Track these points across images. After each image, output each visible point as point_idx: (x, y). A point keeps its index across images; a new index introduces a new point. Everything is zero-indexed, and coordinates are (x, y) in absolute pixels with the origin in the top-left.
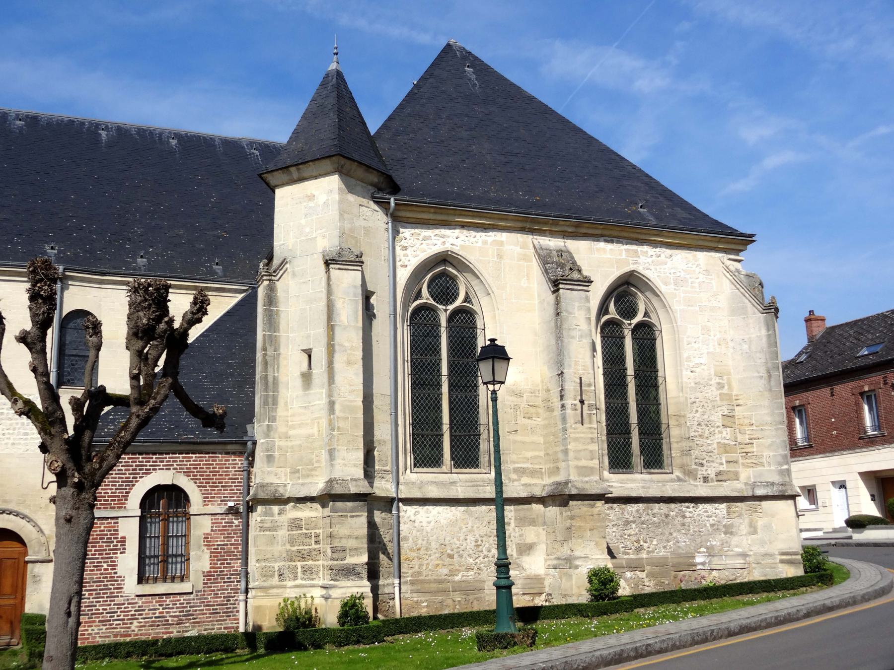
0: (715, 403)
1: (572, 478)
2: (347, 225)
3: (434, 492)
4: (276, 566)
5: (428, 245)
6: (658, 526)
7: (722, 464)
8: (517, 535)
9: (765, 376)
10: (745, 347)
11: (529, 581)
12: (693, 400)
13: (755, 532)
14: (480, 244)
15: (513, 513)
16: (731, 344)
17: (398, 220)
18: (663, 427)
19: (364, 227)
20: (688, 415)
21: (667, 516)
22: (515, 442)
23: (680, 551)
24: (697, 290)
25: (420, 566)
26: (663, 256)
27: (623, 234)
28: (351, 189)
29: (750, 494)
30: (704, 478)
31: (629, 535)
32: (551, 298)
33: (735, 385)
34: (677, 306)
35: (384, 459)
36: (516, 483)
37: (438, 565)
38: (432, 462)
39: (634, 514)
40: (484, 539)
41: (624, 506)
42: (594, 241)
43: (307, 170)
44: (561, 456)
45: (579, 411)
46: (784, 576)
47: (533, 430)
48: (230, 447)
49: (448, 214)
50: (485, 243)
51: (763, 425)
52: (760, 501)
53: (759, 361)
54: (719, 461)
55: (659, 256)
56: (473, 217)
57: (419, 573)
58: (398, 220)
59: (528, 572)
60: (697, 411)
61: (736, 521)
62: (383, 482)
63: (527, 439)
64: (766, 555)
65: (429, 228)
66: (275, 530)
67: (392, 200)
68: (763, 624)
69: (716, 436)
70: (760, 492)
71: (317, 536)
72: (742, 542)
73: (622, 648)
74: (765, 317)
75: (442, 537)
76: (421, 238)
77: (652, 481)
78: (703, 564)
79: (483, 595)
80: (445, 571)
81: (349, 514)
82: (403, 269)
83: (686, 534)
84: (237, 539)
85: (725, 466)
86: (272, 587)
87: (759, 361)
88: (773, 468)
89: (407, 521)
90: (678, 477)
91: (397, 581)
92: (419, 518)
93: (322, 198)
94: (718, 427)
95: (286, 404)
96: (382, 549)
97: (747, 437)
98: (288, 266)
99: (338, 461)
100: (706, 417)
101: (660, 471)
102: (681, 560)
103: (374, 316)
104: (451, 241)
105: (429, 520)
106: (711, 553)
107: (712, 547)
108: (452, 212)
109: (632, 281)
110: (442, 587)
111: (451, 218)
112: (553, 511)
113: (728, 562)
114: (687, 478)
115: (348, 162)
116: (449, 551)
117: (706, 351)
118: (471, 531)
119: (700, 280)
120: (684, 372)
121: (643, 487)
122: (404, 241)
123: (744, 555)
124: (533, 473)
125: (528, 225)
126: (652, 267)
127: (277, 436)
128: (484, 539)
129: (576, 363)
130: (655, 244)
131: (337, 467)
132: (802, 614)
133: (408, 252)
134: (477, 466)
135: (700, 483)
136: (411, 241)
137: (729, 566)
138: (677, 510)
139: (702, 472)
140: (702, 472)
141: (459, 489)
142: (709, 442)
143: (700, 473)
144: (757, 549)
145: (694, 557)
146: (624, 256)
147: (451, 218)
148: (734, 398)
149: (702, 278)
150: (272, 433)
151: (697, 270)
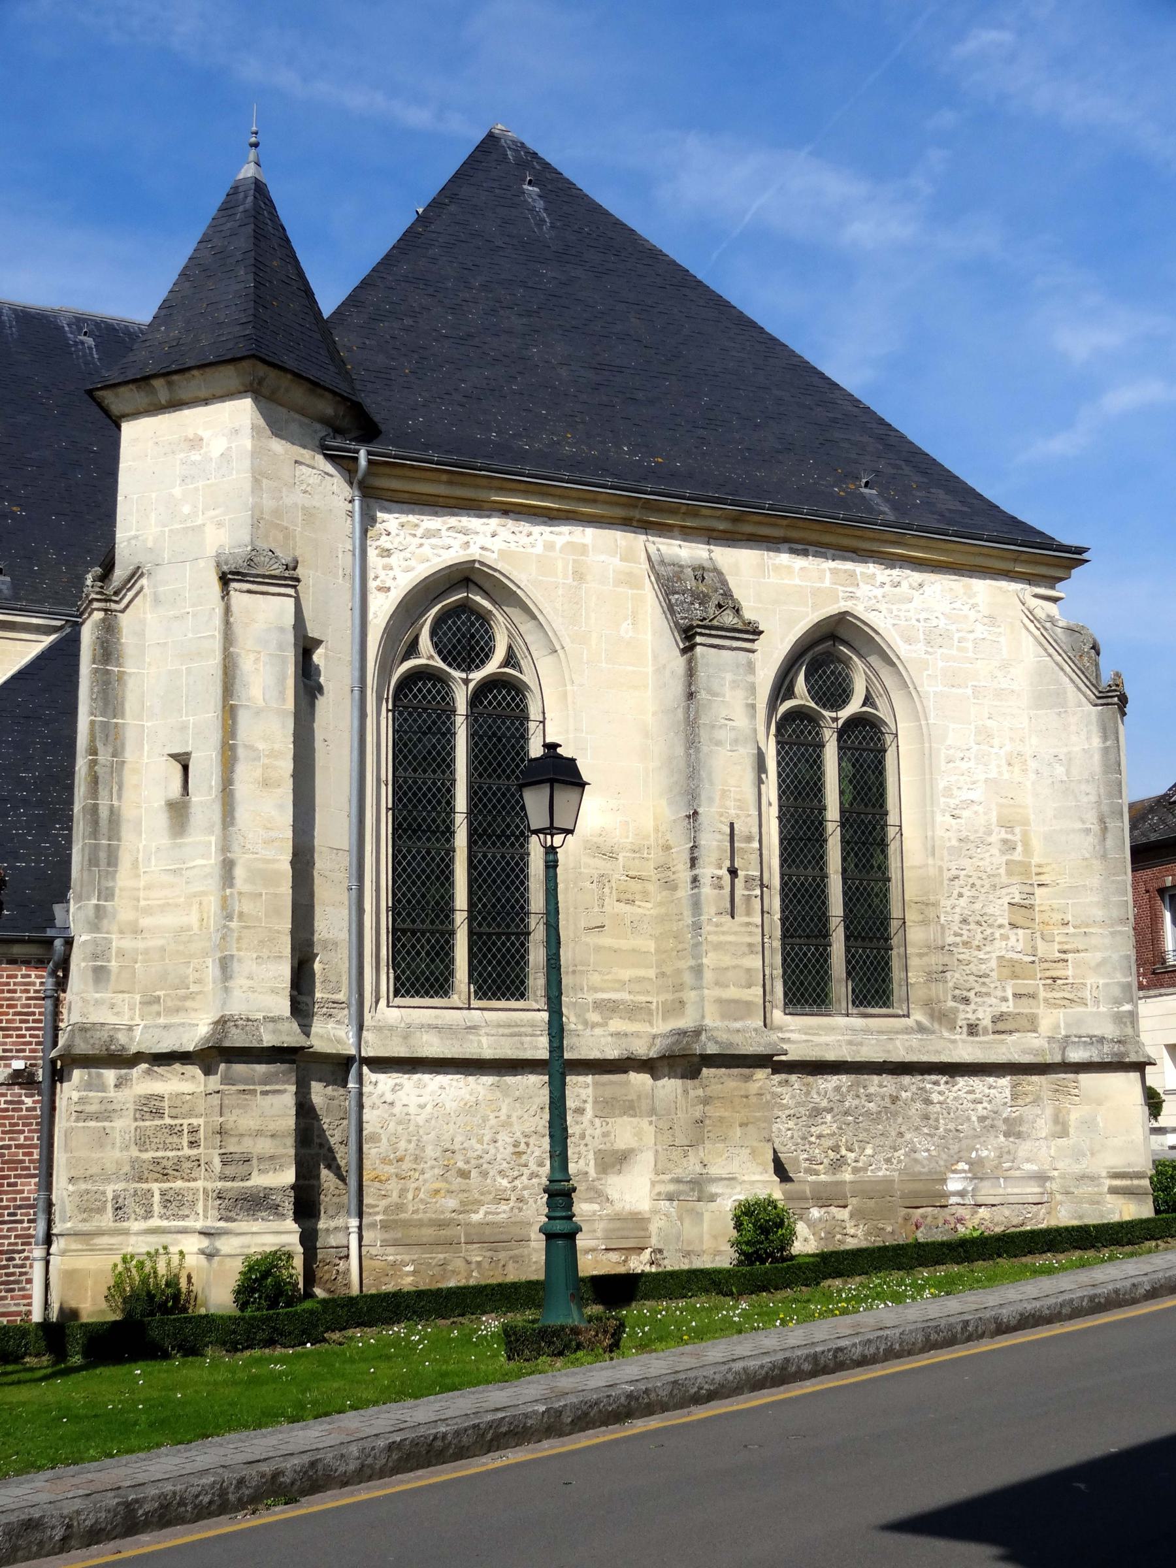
0: (997, 880)
1: (708, 1022)
2: (268, 503)
3: (432, 1047)
4: (110, 1190)
5: (433, 547)
6: (875, 1118)
7: (1005, 999)
8: (598, 1132)
9: (1096, 828)
10: (1060, 770)
11: (618, 1224)
12: (954, 872)
13: (1064, 1133)
14: (539, 549)
15: (590, 1091)
16: (1033, 765)
17: (373, 495)
18: (894, 924)
19: (304, 508)
20: (943, 903)
21: (895, 1099)
22: (598, 949)
23: (918, 1168)
24: (970, 654)
25: (403, 1192)
26: (905, 584)
27: (827, 538)
28: (277, 429)
29: (1057, 1059)
30: (970, 1026)
31: (819, 1137)
33: (1036, 843)
34: (929, 685)
35: (333, 979)
36: (598, 1031)
37: (437, 1192)
38: (432, 986)
39: (831, 1094)
40: (532, 1141)
41: (810, 1079)
42: (769, 550)
44: (688, 978)
45: (728, 889)
46: (1115, 1218)
47: (634, 927)
48: (17, 950)
49: (477, 487)
50: (550, 546)
51: (1087, 926)
52: (1077, 1072)
53: (1085, 799)
54: (999, 993)
55: (898, 585)
56: (526, 493)
57: (400, 1207)
58: (373, 495)
59: (618, 1207)
60: (961, 895)
61: (1029, 1112)
62: (331, 1025)
63: (624, 944)
64: (1083, 1177)
65: (436, 514)
66: (109, 1119)
67: (362, 454)
69: (997, 944)
71: (194, 1131)
72: (1039, 1152)
73: (788, 1354)
74: (1101, 713)
75: (447, 1136)
76: (419, 532)
77: (867, 1031)
78: (962, 1194)
79: (526, 1252)
80: (452, 1203)
81: (259, 1088)
82: (381, 596)
83: (931, 1136)
84: (30, 1136)
85: (1011, 1003)
86: (101, 1233)
87: (1085, 799)
88: (1102, 1009)
89: (378, 1102)
90: (918, 1023)
91: (354, 1223)
92: (402, 1097)
93: (217, 446)
94: (1000, 926)
95: (135, 864)
96: (325, 1159)
97: (1057, 947)
98: (144, 581)
99: (239, 982)
100: (978, 906)
101: (884, 1011)
102: (919, 1186)
103: (320, 689)
104: (481, 540)
105: (422, 1100)
106: (978, 1171)
107: (980, 1161)
108: (485, 482)
109: (842, 633)
110: (444, 1235)
111: (481, 495)
112: (670, 1087)
113: (1009, 1190)
114: (936, 1026)
115: (272, 374)
116: (460, 1164)
117: (982, 777)
118: (507, 1124)
119: (977, 635)
120: (939, 818)
121: (850, 1043)
122: (384, 538)
123: (1041, 1178)
124: (633, 1011)
125: (636, 514)
126: (883, 607)
127: (115, 928)
128: (532, 1141)
129: (724, 792)
130: (891, 561)
131: (237, 993)
132: (1141, 1291)
133: (393, 561)
134: (522, 996)
135: (961, 1036)
136: (401, 538)
137: (1012, 1199)
138: (914, 1088)
139: (965, 1015)
140: (965, 1015)
141: (484, 1040)
142: (981, 955)
143: (962, 1016)
144: (1067, 1166)
145: (944, 1181)
146: (827, 583)
147: (481, 495)
148: (1034, 870)
149: (980, 630)
150: (105, 922)
151: (973, 615)
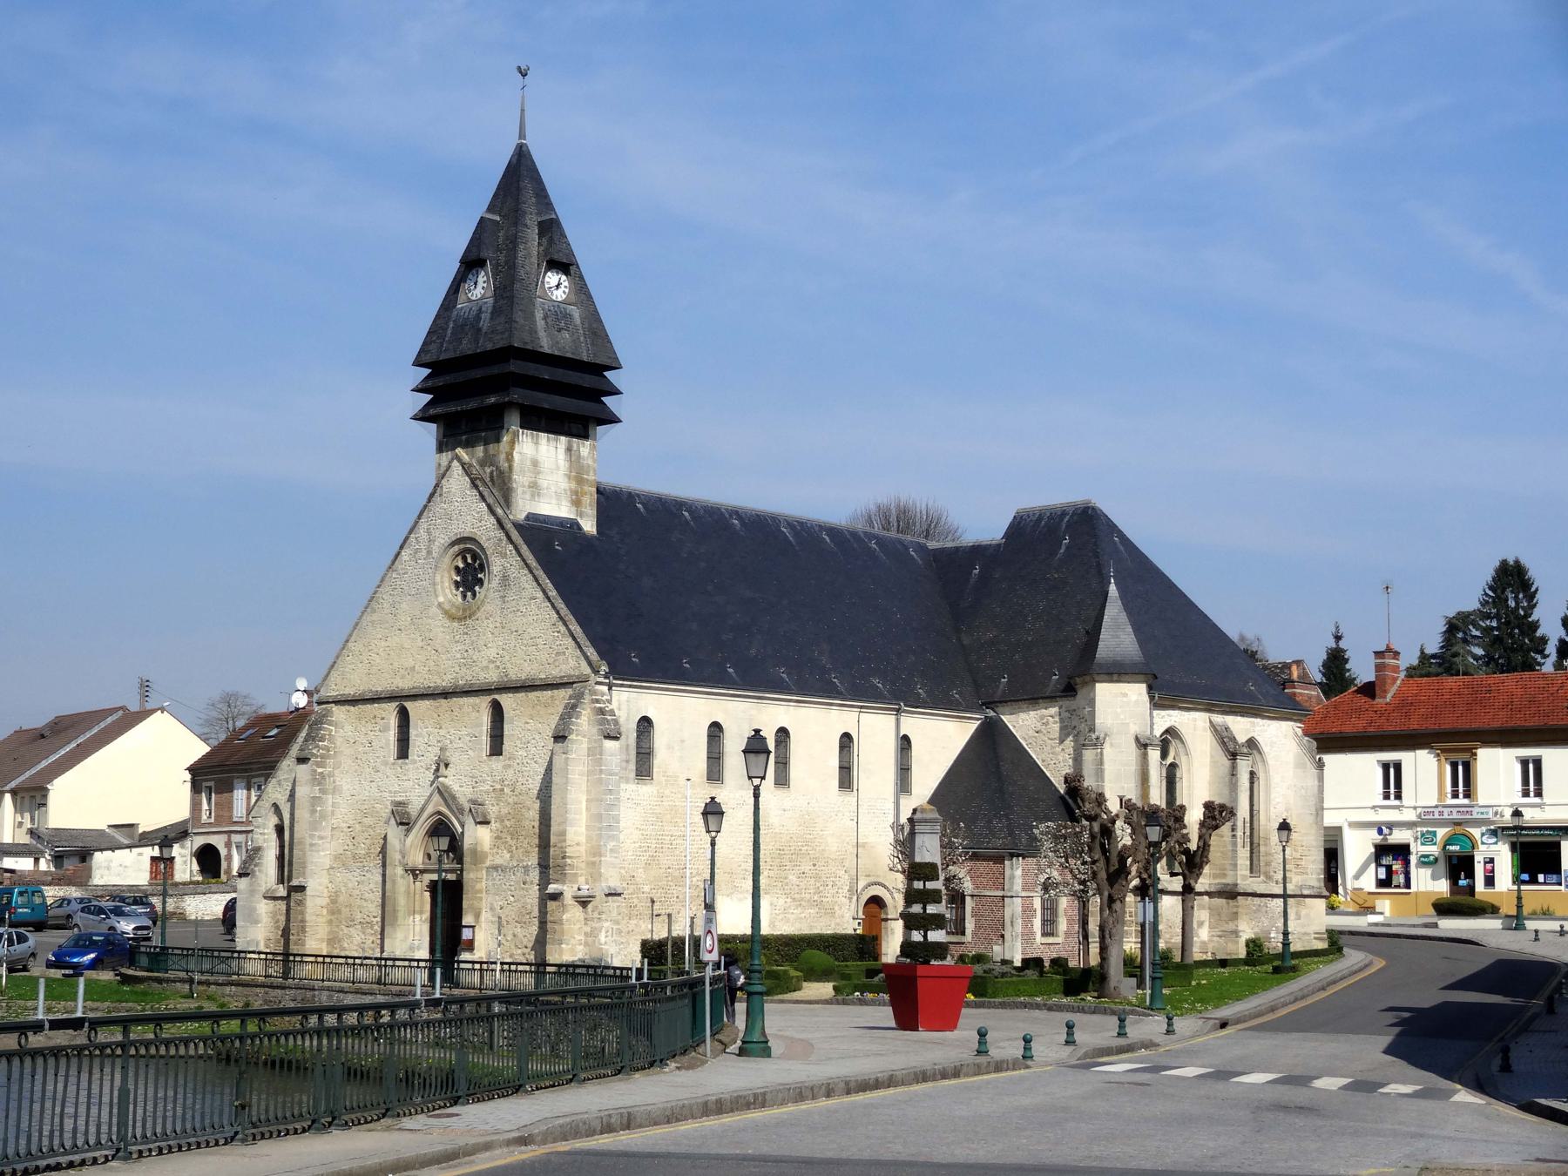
17: (1156, 704)
32: (1225, 762)
68: (583, 1128)
70: (1306, 892)
93: (1134, 698)
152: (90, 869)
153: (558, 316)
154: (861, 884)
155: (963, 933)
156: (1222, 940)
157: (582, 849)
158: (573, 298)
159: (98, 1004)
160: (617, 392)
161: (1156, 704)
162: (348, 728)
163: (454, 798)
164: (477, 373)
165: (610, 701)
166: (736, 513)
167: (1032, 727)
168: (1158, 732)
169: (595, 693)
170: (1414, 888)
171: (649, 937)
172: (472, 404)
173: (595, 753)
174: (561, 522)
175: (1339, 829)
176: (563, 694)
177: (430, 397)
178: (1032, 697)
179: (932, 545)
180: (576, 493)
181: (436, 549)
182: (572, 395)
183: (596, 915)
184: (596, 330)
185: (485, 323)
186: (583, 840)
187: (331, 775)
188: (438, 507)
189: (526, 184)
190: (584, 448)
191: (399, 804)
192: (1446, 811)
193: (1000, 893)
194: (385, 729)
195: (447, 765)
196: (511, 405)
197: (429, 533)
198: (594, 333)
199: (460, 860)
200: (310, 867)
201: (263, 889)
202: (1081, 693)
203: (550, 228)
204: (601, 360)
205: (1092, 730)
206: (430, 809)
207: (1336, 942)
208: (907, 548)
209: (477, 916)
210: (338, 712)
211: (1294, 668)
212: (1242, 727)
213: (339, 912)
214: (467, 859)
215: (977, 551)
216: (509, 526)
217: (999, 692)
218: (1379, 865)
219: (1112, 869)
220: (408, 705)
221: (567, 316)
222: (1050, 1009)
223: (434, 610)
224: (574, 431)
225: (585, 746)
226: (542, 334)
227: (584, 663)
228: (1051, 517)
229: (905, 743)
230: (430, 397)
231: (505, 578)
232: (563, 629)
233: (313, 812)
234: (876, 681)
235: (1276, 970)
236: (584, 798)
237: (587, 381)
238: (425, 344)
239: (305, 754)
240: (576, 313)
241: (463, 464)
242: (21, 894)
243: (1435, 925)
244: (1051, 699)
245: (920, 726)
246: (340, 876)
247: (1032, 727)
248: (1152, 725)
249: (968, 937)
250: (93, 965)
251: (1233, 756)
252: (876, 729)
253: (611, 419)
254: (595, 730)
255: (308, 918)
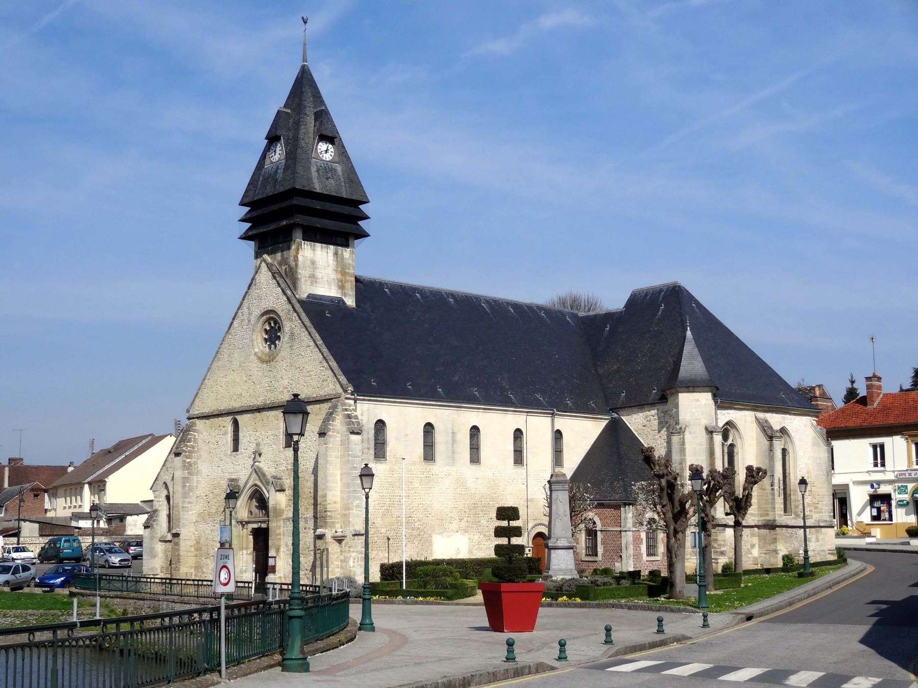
32: (768, 443)
43: (697, 389)
70: (822, 524)
93: (703, 402)
112: (763, 531)
130: (790, 414)
144: (818, 548)
152: (125, 526)
153: (327, 170)
154: (531, 525)
155: (596, 555)
156: (767, 556)
157: (338, 506)
158: (337, 159)
159: (35, 611)
160: (365, 217)
161: (720, 406)
162: (205, 433)
163: (264, 475)
164: (275, 207)
165: (355, 410)
166: (452, 295)
167: (641, 424)
168: (721, 424)
169: (345, 404)
170: (894, 521)
171: (386, 561)
172: (272, 227)
173: (345, 444)
174: (331, 299)
175: (847, 485)
176: (326, 406)
177: (248, 225)
178: (640, 404)
179: (581, 314)
180: (341, 281)
181: (253, 319)
182: (339, 220)
183: (347, 549)
184: (352, 178)
185: (280, 176)
186: (338, 499)
187: (195, 463)
188: (254, 292)
189: (308, 91)
190: (346, 253)
191: (232, 480)
192: (913, 473)
193: (618, 529)
194: (225, 433)
195: (260, 455)
196: (295, 226)
197: (249, 309)
198: (351, 181)
199: (267, 514)
200: (182, 521)
201: (159, 536)
202: (671, 400)
203: (322, 115)
204: (355, 197)
205: (677, 423)
206: (250, 483)
207: (842, 555)
208: (564, 316)
209: (278, 551)
210: (200, 424)
211: (817, 389)
212: (776, 420)
213: (201, 549)
214: (271, 514)
215: (609, 317)
216: (294, 301)
217: (620, 402)
218: (872, 507)
219: (676, 511)
220: (238, 417)
221: (333, 170)
222: (629, 608)
223: (253, 357)
224: (339, 240)
225: (339, 439)
226: (315, 180)
227: (338, 386)
228: (653, 294)
229: (558, 435)
230: (248, 225)
231: (292, 334)
232: (325, 364)
233: (184, 486)
234: (538, 396)
235: (801, 575)
236: (338, 474)
237: (346, 210)
238: (246, 191)
239: (179, 451)
240: (339, 168)
241: (267, 264)
242: (65, 541)
243: (908, 543)
244: (652, 405)
245: (565, 423)
246: (202, 526)
247: (641, 424)
248: (717, 419)
249: (600, 558)
250: (63, 585)
251: (771, 438)
252: (538, 427)
253: (363, 235)
254: (344, 429)
255: (181, 553)
